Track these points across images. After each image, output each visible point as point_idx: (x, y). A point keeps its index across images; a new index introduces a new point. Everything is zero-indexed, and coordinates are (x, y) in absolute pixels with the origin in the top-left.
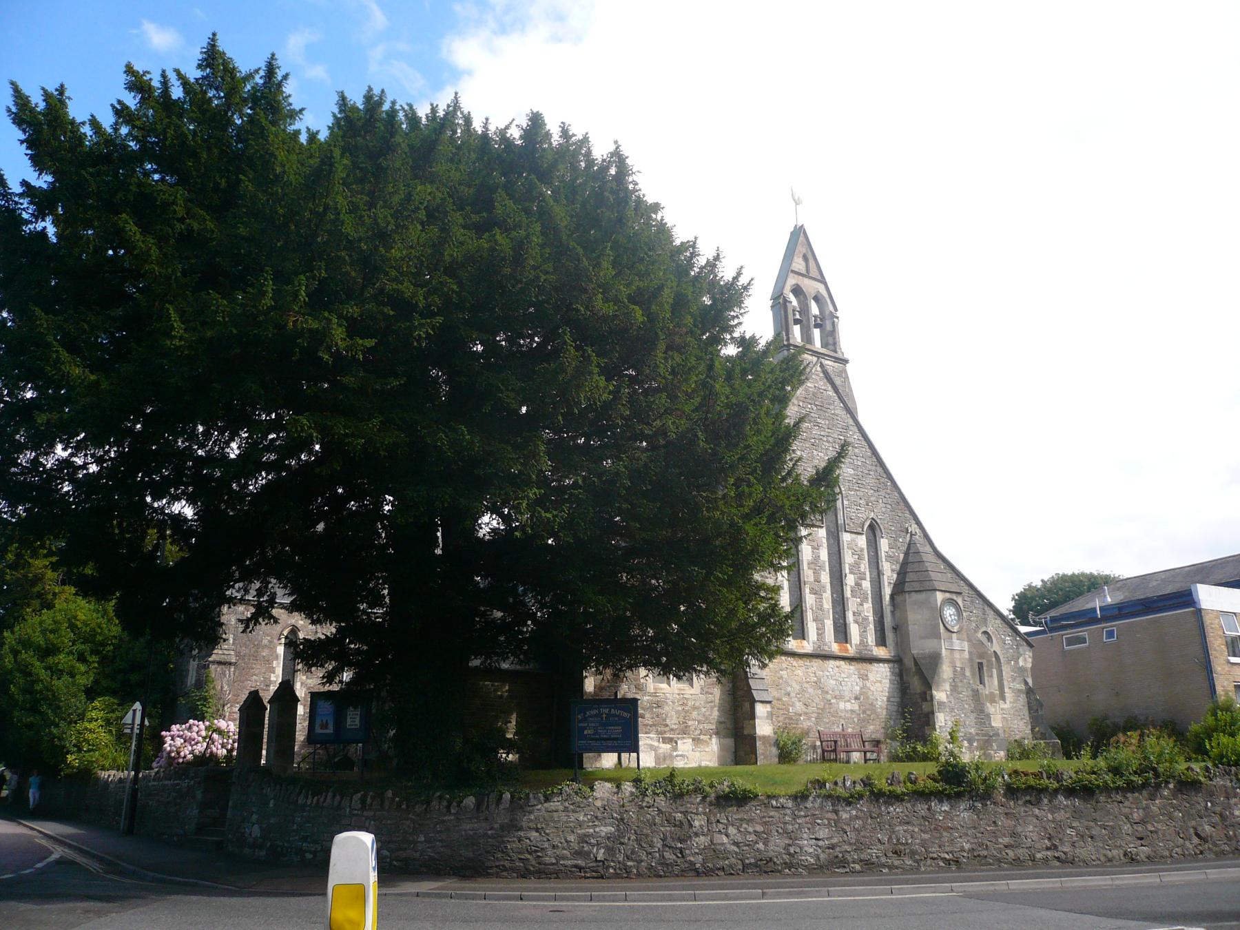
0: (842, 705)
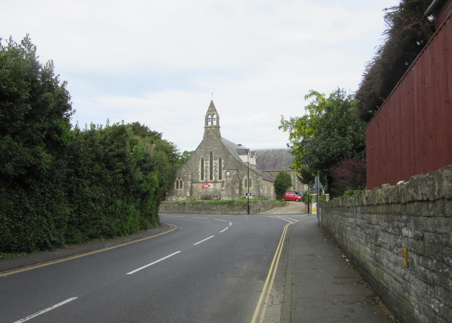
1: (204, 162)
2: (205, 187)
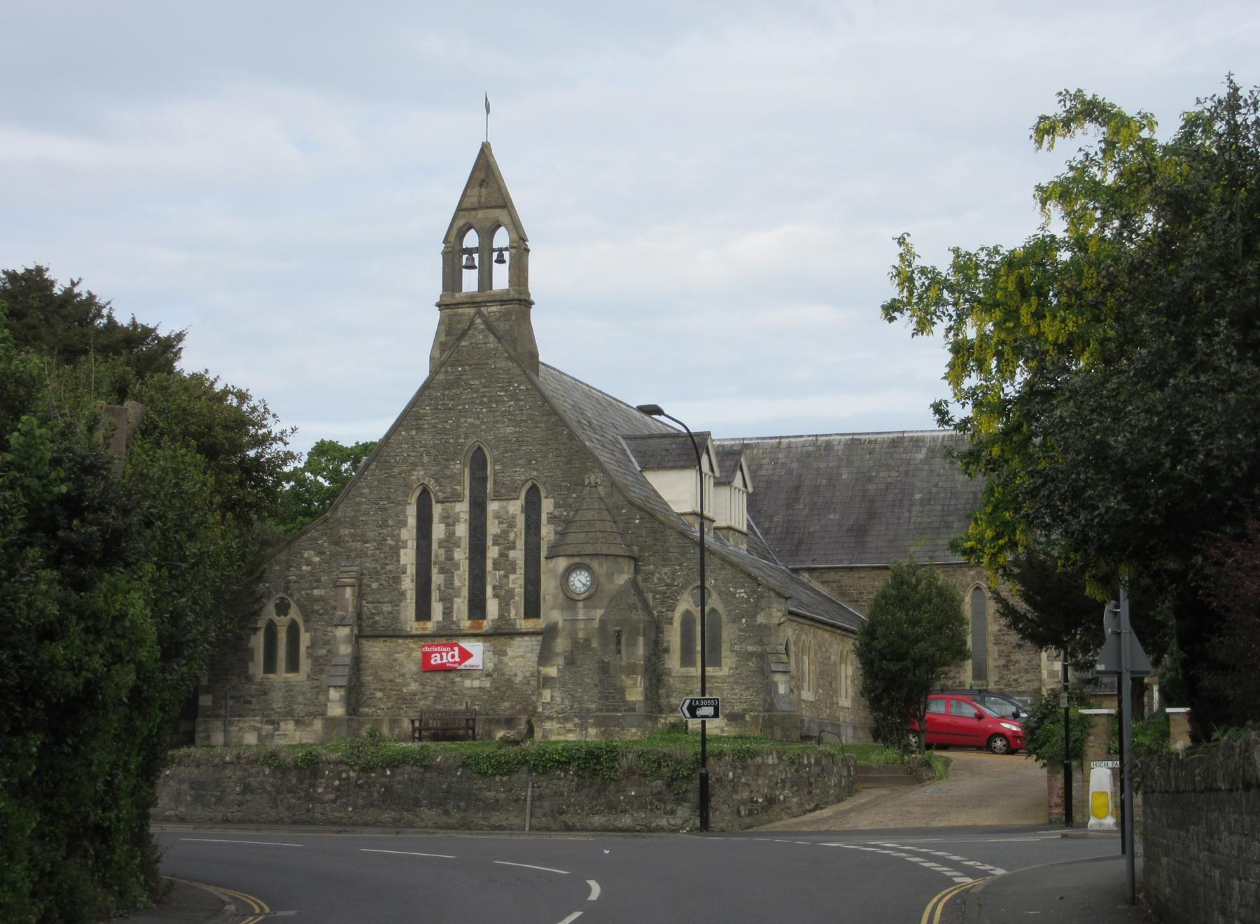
0: (468, 683)
1: (437, 510)
2: (436, 660)
